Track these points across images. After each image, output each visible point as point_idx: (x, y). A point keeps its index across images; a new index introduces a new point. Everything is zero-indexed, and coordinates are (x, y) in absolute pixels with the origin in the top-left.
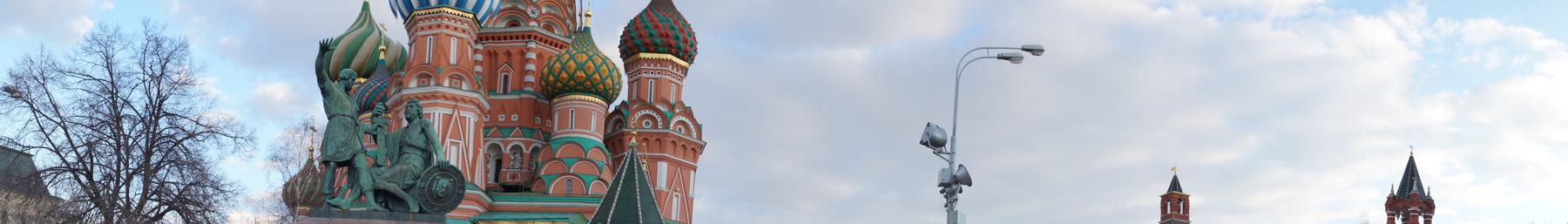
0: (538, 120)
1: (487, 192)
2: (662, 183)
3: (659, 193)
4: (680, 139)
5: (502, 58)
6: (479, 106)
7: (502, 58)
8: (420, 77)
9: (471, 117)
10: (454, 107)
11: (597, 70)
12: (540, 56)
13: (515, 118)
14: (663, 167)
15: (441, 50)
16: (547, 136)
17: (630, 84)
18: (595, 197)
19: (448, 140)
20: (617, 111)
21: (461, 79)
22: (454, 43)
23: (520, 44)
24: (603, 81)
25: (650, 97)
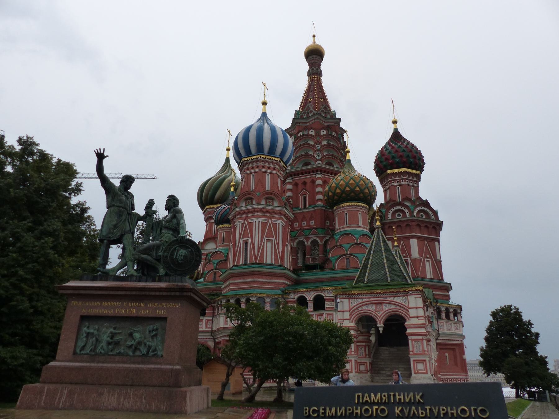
1: (295, 271)
2: (415, 252)
3: (414, 261)
4: (423, 222)
6: (285, 216)
7: (300, 186)
8: (246, 199)
9: (280, 224)
12: (325, 182)
13: (313, 223)
14: (414, 243)
17: (385, 191)
19: (265, 239)
21: (273, 199)
22: (268, 178)
24: (362, 191)
25: (399, 198)
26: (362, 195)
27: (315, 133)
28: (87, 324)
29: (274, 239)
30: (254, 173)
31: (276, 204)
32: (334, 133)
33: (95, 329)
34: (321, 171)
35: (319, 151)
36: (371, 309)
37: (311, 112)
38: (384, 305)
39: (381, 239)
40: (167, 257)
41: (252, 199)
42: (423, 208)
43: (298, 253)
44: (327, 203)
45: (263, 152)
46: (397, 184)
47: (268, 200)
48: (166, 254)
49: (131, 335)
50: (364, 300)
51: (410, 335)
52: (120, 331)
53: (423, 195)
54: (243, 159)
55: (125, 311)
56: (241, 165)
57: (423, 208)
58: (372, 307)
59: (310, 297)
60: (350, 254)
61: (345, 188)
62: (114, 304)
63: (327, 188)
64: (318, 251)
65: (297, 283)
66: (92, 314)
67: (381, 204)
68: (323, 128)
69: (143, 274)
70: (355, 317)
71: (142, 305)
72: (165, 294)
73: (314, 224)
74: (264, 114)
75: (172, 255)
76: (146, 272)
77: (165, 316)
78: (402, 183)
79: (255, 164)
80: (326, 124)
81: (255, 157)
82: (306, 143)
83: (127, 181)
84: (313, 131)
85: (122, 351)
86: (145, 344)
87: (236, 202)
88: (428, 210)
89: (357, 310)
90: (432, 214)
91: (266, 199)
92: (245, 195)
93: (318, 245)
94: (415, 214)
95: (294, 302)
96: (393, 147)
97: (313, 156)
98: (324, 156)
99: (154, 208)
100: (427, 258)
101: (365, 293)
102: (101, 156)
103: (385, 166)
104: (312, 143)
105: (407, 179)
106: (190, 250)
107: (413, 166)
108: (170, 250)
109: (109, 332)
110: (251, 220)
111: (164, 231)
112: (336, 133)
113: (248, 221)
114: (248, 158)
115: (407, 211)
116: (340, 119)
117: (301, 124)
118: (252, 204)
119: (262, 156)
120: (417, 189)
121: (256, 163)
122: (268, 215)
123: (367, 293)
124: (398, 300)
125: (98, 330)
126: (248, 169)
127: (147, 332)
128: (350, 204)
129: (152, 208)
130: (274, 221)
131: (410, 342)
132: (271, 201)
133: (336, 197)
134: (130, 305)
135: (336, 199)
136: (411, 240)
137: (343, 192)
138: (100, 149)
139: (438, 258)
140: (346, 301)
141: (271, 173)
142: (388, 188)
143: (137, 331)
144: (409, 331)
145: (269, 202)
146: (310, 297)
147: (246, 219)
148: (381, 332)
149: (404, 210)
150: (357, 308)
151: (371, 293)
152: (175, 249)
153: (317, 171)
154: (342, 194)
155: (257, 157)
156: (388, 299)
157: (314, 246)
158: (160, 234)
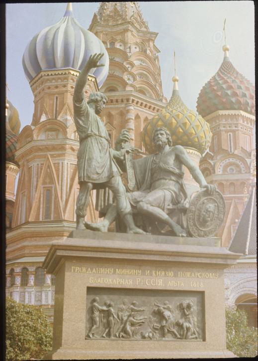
33: (110, 306)
49: (159, 315)
54: (42, 73)
67: (207, 153)
68: (136, 44)
71: (171, 274)
79: (59, 82)
85: (151, 335)
86: (180, 326)
96: (226, 82)
106: (216, 204)
107: (249, 109)
108: (197, 203)
116: (157, 34)
119: (72, 72)
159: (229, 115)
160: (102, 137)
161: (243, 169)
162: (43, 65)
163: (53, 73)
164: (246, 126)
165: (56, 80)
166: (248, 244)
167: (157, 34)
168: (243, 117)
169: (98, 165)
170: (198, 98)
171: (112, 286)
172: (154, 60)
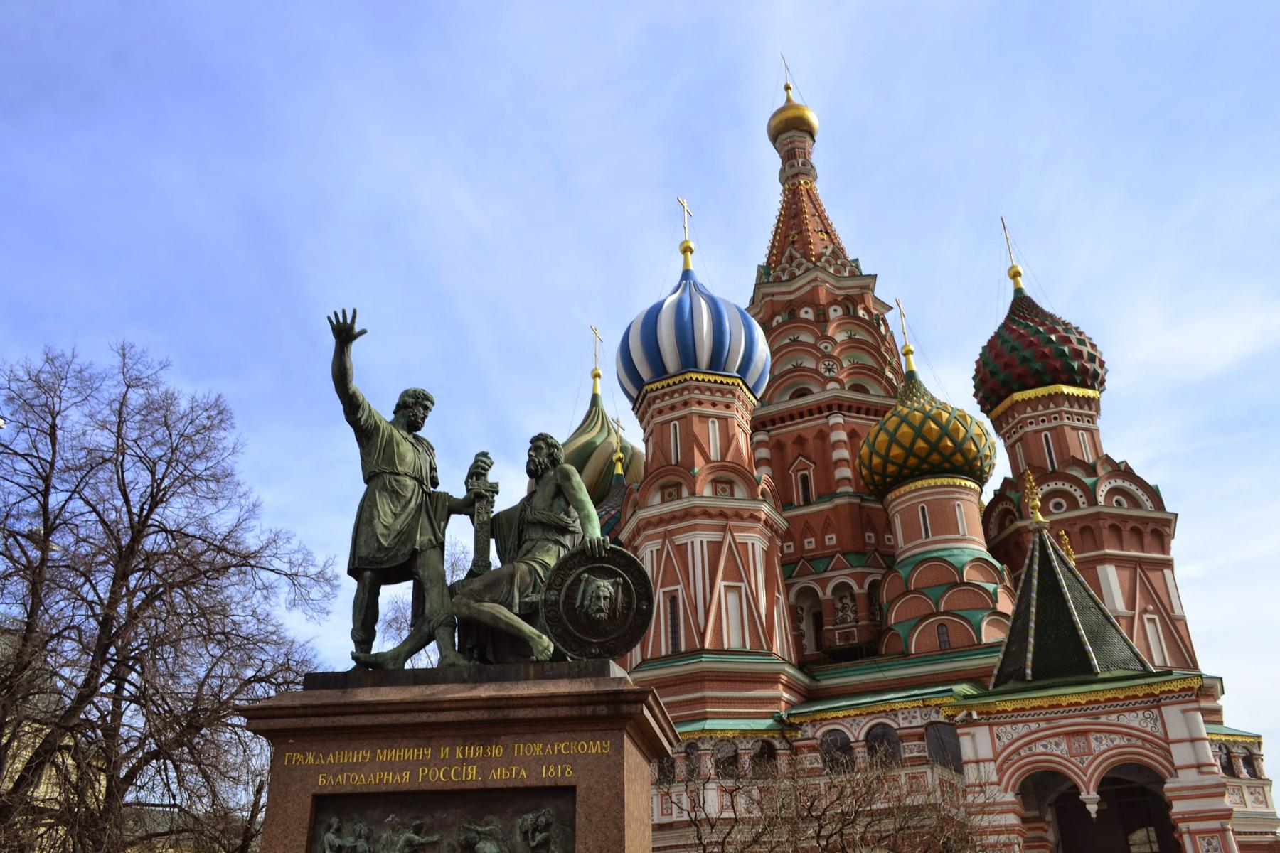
0: (870, 537)
1: (802, 665)
5: (790, 449)
8: (663, 488)
9: (756, 541)
10: (724, 529)
11: (945, 431)
12: (853, 435)
13: (831, 539)
14: (1111, 576)
15: (691, 441)
16: (889, 560)
17: (1010, 449)
18: (993, 647)
19: (720, 584)
20: (999, 496)
21: (731, 483)
23: (815, 423)
25: (1050, 461)
26: (959, 457)
27: (816, 315)
28: (335, 821)
29: (743, 585)
30: (678, 419)
31: (740, 492)
32: (861, 313)
33: (360, 836)
34: (840, 407)
35: (830, 357)
36: (1055, 752)
37: (799, 266)
38: (1092, 737)
39: (1054, 557)
40: (557, 602)
41: (678, 485)
42: (1119, 483)
43: (800, 620)
44: (866, 484)
45: (696, 365)
46: (1042, 426)
47: (720, 486)
48: (553, 595)
50: (1034, 726)
51: (1184, 820)
52: (436, 838)
53: (1115, 448)
55: (447, 774)
56: (641, 404)
57: (1119, 483)
58: (1057, 744)
59: (857, 732)
60: (946, 613)
61: (914, 442)
62: (410, 754)
63: (865, 450)
64: (856, 612)
65: (810, 696)
66: (349, 789)
67: (1006, 480)
69: (483, 659)
70: (1013, 776)
71: (496, 751)
72: (563, 712)
73: (834, 542)
74: (686, 274)
75: (571, 596)
76: (491, 657)
77: (566, 783)
78: (1054, 423)
79: (677, 399)
80: (838, 292)
81: (676, 380)
82: (795, 341)
83: (415, 404)
84: (810, 310)
87: (636, 496)
88: (1133, 488)
89: (1016, 757)
90: (1145, 498)
91: (715, 482)
92: (659, 476)
93: (853, 597)
94: (1101, 499)
95: (812, 749)
97: (817, 371)
98: (842, 367)
99: (491, 477)
100: (1151, 613)
101: (1033, 708)
102: (345, 334)
103: (1004, 383)
104: (811, 340)
105: (1067, 412)
108: (563, 581)
109: (401, 842)
110: (680, 539)
111: (535, 534)
112: (867, 310)
113: (672, 542)
114: (659, 385)
115: (1078, 494)
116: (874, 277)
117: (776, 298)
118: (679, 497)
119: (694, 376)
120: (1093, 433)
121: (681, 395)
122: (723, 522)
123: (1041, 708)
124: (1133, 720)
125: (368, 839)
126: (660, 412)
127: (518, 837)
128: (932, 482)
129: (484, 475)
130: (740, 537)
131: (1187, 840)
132: (727, 487)
133: (891, 468)
134: (458, 754)
135: (882, 480)
136: (1099, 568)
137: (909, 451)
138: (344, 312)
139: (1177, 612)
140: (982, 733)
141: (718, 418)
142: (1020, 439)
143: (488, 836)
144: (1178, 807)
145: (724, 490)
146: (857, 732)
147: (668, 535)
148: (1094, 815)
149: (1072, 490)
150: (1017, 751)
151: (1051, 706)
152: (578, 580)
153: (830, 408)
154: (906, 459)
155: (681, 378)
156: (1103, 719)
157: (841, 599)
158: (520, 547)
159: (1037, 398)
160: (398, 474)
161: (1081, 500)
162: (644, 371)
163: (665, 383)
164: (1077, 414)
165: (671, 395)
166: (1030, 656)
167: (874, 277)
168: (1068, 397)
169: (385, 532)
170: (974, 378)
171: (365, 790)
172: (875, 324)
